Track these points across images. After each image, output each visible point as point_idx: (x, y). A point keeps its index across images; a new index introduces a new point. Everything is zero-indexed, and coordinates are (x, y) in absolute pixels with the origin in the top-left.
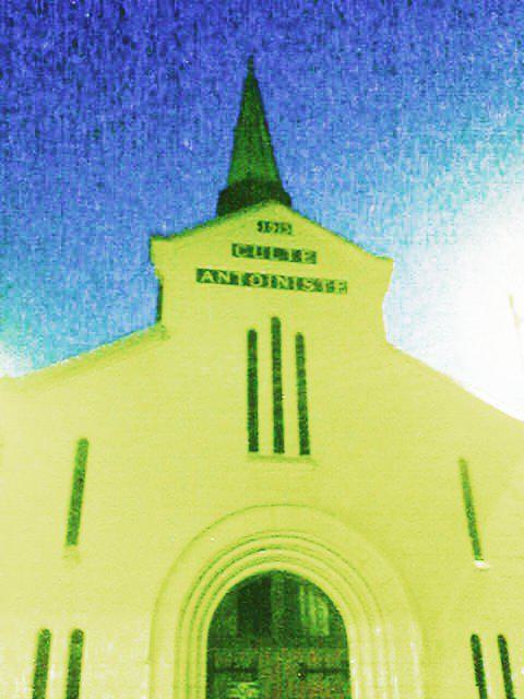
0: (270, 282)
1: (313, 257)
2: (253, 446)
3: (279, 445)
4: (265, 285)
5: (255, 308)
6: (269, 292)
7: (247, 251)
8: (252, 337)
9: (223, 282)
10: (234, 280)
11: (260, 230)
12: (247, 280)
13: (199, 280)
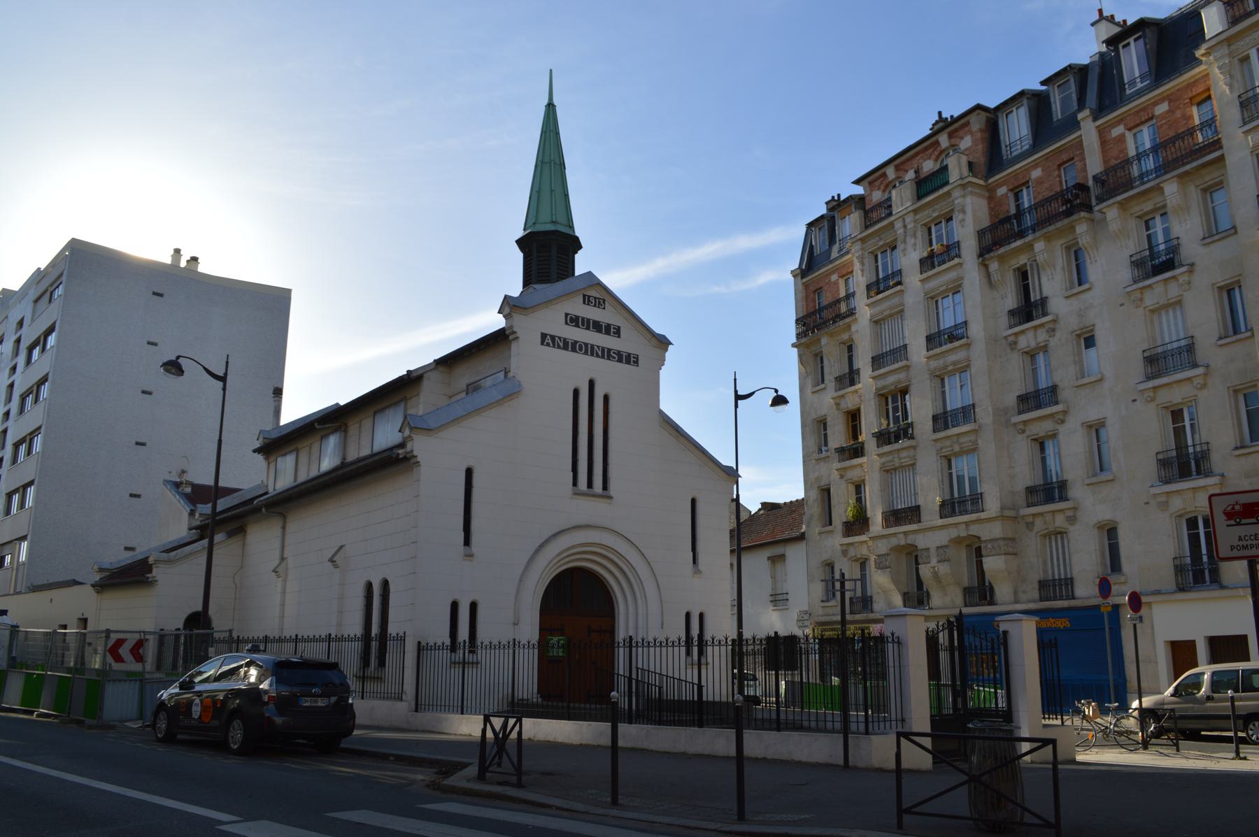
0: (589, 350)
1: (618, 333)
2: (575, 484)
3: (590, 485)
4: (586, 353)
5: (580, 369)
6: (588, 359)
7: (574, 321)
8: (576, 393)
9: (559, 347)
10: (565, 348)
12: (573, 346)
13: (542, 343)
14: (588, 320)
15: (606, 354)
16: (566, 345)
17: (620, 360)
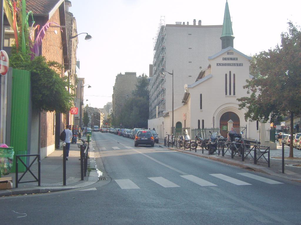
0: (229, 65)
1: (237, 59)
2: (226, 94)
3: (230, 94)
4: (228, 65)
5: (226, 70)
6: (229, 67)
8: (226, 75)
9: (221, 65)
10: (223, 65)
11: (228, 54)
13: (217, 66)
14: (229, 58)
15: (234, 65)
16: (223, 65)
17: (238, 66)
